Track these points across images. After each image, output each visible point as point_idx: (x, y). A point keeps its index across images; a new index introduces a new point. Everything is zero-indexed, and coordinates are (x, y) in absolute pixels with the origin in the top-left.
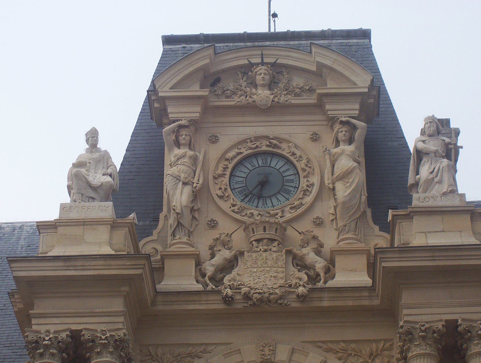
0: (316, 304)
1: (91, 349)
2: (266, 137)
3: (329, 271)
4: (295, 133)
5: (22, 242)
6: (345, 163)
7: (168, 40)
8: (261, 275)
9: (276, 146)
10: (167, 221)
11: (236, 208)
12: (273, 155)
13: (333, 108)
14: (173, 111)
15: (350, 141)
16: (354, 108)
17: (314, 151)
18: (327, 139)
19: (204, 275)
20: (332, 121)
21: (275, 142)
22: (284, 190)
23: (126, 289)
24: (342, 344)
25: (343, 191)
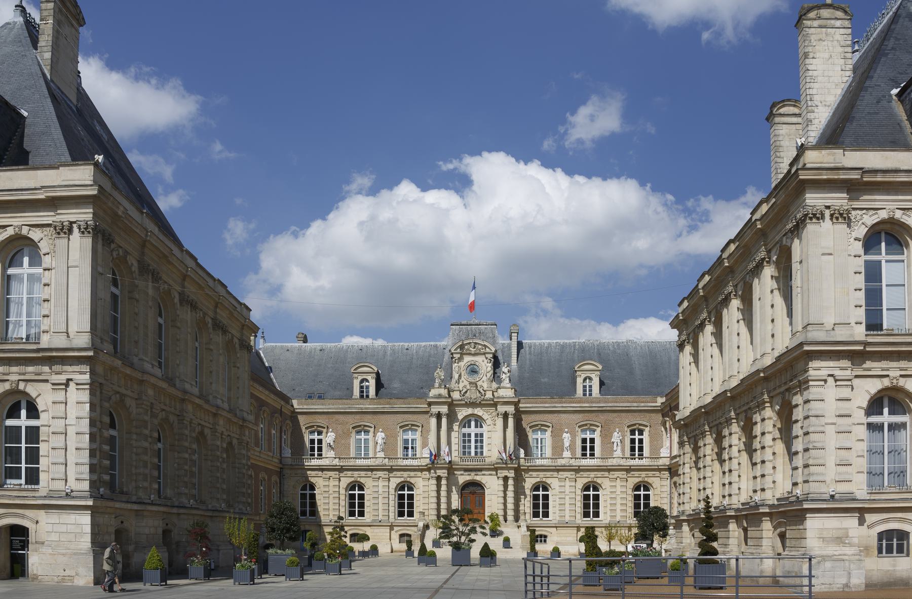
4: (480, 359)
6: (489, 369)
8: (473, 395)
10: (454, 381)
16: (491, 355)
17: (483, 364)
25: (489, 375)
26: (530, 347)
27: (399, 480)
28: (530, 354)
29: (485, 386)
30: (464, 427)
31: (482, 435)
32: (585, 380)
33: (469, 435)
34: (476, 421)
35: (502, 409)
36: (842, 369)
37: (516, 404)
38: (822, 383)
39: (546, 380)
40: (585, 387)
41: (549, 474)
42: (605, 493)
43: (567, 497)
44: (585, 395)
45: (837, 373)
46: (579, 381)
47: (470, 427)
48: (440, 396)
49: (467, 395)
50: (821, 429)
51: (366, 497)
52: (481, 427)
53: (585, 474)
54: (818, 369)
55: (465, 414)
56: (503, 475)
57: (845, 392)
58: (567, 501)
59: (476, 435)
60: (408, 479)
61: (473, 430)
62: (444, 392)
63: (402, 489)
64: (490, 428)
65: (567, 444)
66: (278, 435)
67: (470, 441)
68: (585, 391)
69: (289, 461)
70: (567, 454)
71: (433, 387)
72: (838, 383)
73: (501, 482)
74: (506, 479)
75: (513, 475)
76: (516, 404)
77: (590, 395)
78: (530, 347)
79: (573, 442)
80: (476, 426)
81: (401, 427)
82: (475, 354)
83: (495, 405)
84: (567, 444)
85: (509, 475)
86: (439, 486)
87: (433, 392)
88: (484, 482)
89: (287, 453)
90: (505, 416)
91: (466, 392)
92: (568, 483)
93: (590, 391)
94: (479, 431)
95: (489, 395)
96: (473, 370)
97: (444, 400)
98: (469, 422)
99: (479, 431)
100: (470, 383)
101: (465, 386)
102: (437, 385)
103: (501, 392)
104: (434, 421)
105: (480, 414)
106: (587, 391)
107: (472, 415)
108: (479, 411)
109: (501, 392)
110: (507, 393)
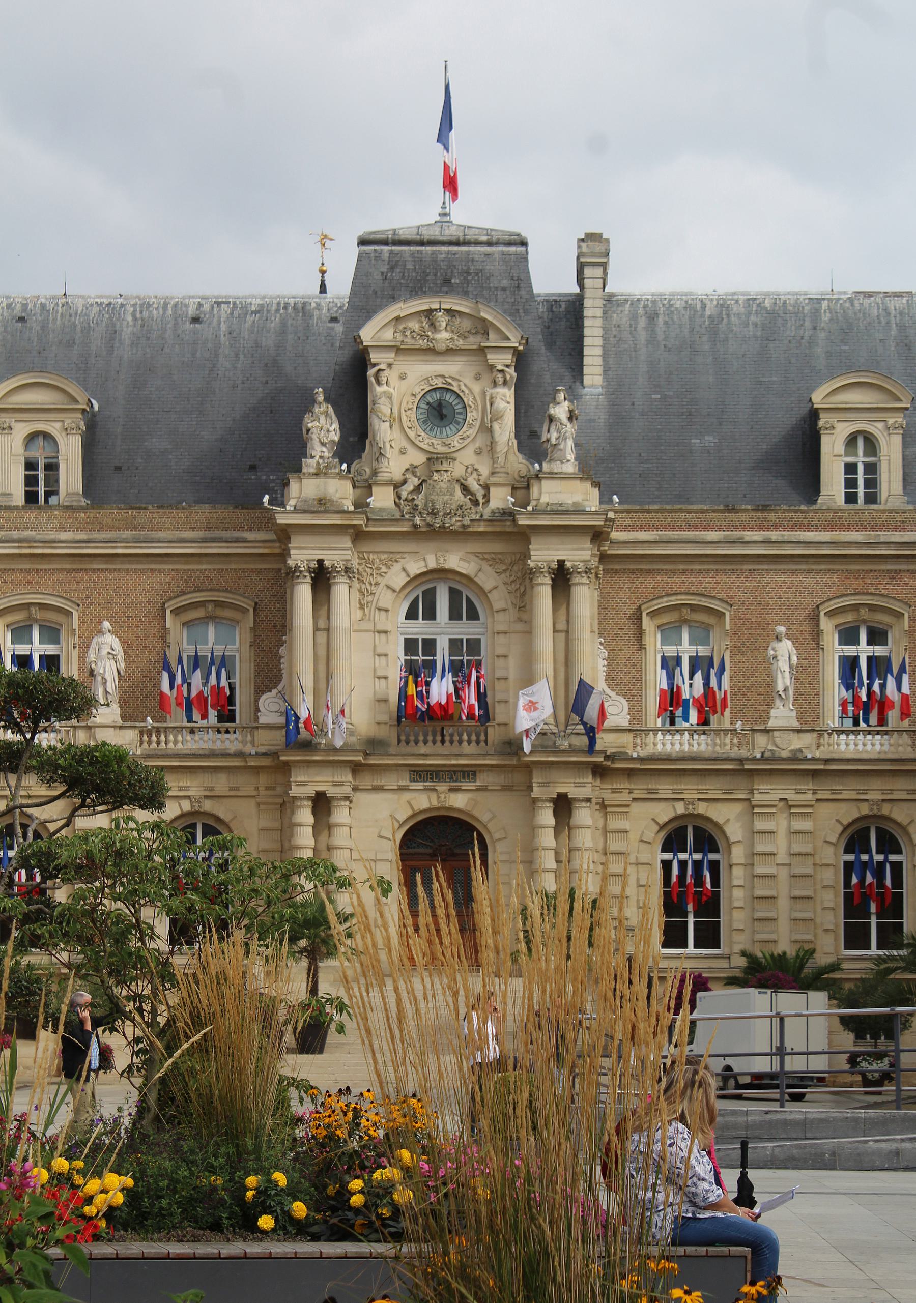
0: (475, 529)
1: (330, 573)
2: (443, 376)
3: (486, 496)
5: (223, 327)
9: (450, 384)
11: (420, 438)
12: (448, 390)
13: (492, 358)
14: (374, 357)
15: (505, 383)
16: (508, 358)
19: (400, 498)
20: (492, 367)
21: (449, 380)
23: (352, 531)
24: (493, 556)
26: (652, 317)
28: (652, 340)
31: (474, 646)
32: (851, 441)
33: (430, 645)
34: (455, 595)
35: (544, 554)
40: (850, 468)
44: (851, 498)
47: (430, 614)
48: (323, 504)
52: (473, 615)
55: (416, 568)
59: (455, 644)
60: (208, 806)
62: (341, 491)
65: (784, 680)
68: (851, 483)
70: (782, 715)
74: (563, 806)
77: (871, 498)
78: (652, 317)
79: (807, 675)
80: (455, 615)
81: (176, 612)
83: (524, 536)
84: (784, 680)
85: (572, 791)
87: (302, 489)
90: (562, 577)
93: (871, 483)
95: (501, 498)
99: (465, 630)
101: (412, 469)
102: (309, 465)
106: (863, 483)
107: (441, 573)
109: (547, 493)
110: (566, 490)
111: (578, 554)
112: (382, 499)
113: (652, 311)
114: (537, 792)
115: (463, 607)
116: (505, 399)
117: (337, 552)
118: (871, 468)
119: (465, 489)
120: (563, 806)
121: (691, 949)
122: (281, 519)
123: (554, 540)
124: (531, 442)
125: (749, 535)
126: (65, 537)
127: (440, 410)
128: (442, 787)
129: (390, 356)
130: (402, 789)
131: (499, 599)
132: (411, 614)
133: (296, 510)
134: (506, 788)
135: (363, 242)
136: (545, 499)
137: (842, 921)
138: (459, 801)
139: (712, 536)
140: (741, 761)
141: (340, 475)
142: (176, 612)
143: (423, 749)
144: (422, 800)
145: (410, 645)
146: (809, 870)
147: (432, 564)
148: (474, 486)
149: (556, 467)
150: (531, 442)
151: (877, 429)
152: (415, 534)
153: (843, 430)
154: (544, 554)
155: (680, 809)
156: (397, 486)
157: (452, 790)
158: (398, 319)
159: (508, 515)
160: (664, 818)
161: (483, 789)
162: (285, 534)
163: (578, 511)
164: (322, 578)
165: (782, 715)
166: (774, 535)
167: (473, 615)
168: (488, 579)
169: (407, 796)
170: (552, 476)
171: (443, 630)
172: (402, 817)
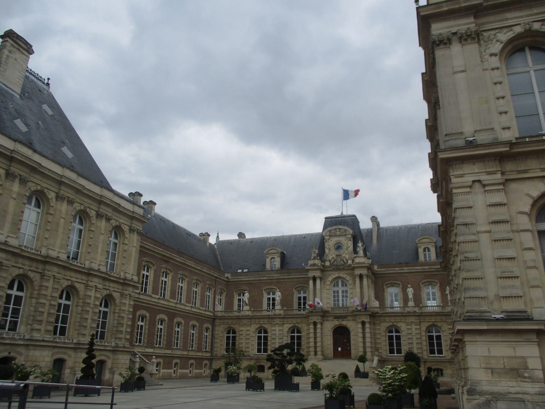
3: (347, 262)
4: (342, 239)
7: (326, 218)
14: (325, 238)
16: (350, 236)
18: (347, 240)
22: (341, 248)
27: (290, 326)
29: (347, 257)
30: (334, 286)
31: (347, 292)
33: (338, 292)
34: (342, 282)
35: (358, 272)
36: (489, 173)
37: (369, 268)
38: (468, 190)
39: (397, 251)
40: (425, 255)
41: (398, 319)
42: (445, 334)
43: (414, 338)
45: (484, 178)
46: (421, 250)
47: (338, 286)
48: (314, 265)
49: (335, 263)
50: (473, 238)
51: (269, 339)
52: (346, 285)
53: (427, 319)
54: (462, 176)
55: (334, 277)
56: (361, 320)
57: (499, 198)
58: (415, 341)
59: (343, 292)
60: (297, 325)
61: (340, 289)
62: (318, 262)
63: (293, 332)
64: (351, 286)
65: (411, 296)
66: (212, 296)
67: (338, 296)
69: (220, 314)
70: (411, 303)
71: (310, 260)
72: (487, 188)
73: (360, 326)
75: (368, 320)
76: (369, 268)
80: (342, 286)
81: (295, 288)
82: (339, 236)
83: (353, 269)
84: (411, 296)
86: (315, 329)
87: (311, 262)
88: (349, 326)
89: (219, 308)
90: (361, 277)
91: (334, 261)
92: (414, 327)
93: (429, 257)
94: (345, 289)
95: (350, 262)
96: (338, 247)
97: (316, 267)
98: (338, 282)
100: (337, 256)
101: (333, 258)
103: (357, 260)
104: (311, 282)
105: (344, 276)
107: (339, 277)
108: (342, 274)
111: (364, 272)
112: (327, 264)
113: (387, 230)
114: (358, 320)
115: (344, 284)
116: (351, 244)
117: (317, 274)
118: (429, 254)
119: (343, 261)
120: (363, 323)
121: (396, 354)
122: (307, 268)
123: (359, 269)
124: (355, 251)
125: (404, 268)
126: (276, 276)
127: (338, 247)
128: (340, 320)
129: (328, 237)
130: (333, 320)
131: (350, 282)
132: (334, 286)
133: (310, 266)
134: (353, 320)
135: (326, 218)
136: (357, 261)
137: (428, 348)
138: (344, 323)
139: (397, 269)
140: (402, 313)
141: (318, 259)
142: (295, 288)
143: (336, 312)
144: (337, 323)
145: (334, 292)
146: (419, 337)
147: (337, 275)
148: (345, 260)
149: (359, 255)
150: (355, 251)
151: (430, 247)
152: (334, 270)
153: (423, 247)
154: (358, 272)
155: (391, 324)
156: (330, 261)
157: (343, 320)
158: (330, 231)
159: (350, 265)
160: (387, 326)
161: (349, 320)
162: (308, 270)
163: (363, 263)
164: (314, 279)
165: (411, 303)
166: (410, 268)
167: (346, 285)
168: (348, 278)
169: (333, 322)
170: (358, 257)
171: (340, 289)
172: (333, 326)
